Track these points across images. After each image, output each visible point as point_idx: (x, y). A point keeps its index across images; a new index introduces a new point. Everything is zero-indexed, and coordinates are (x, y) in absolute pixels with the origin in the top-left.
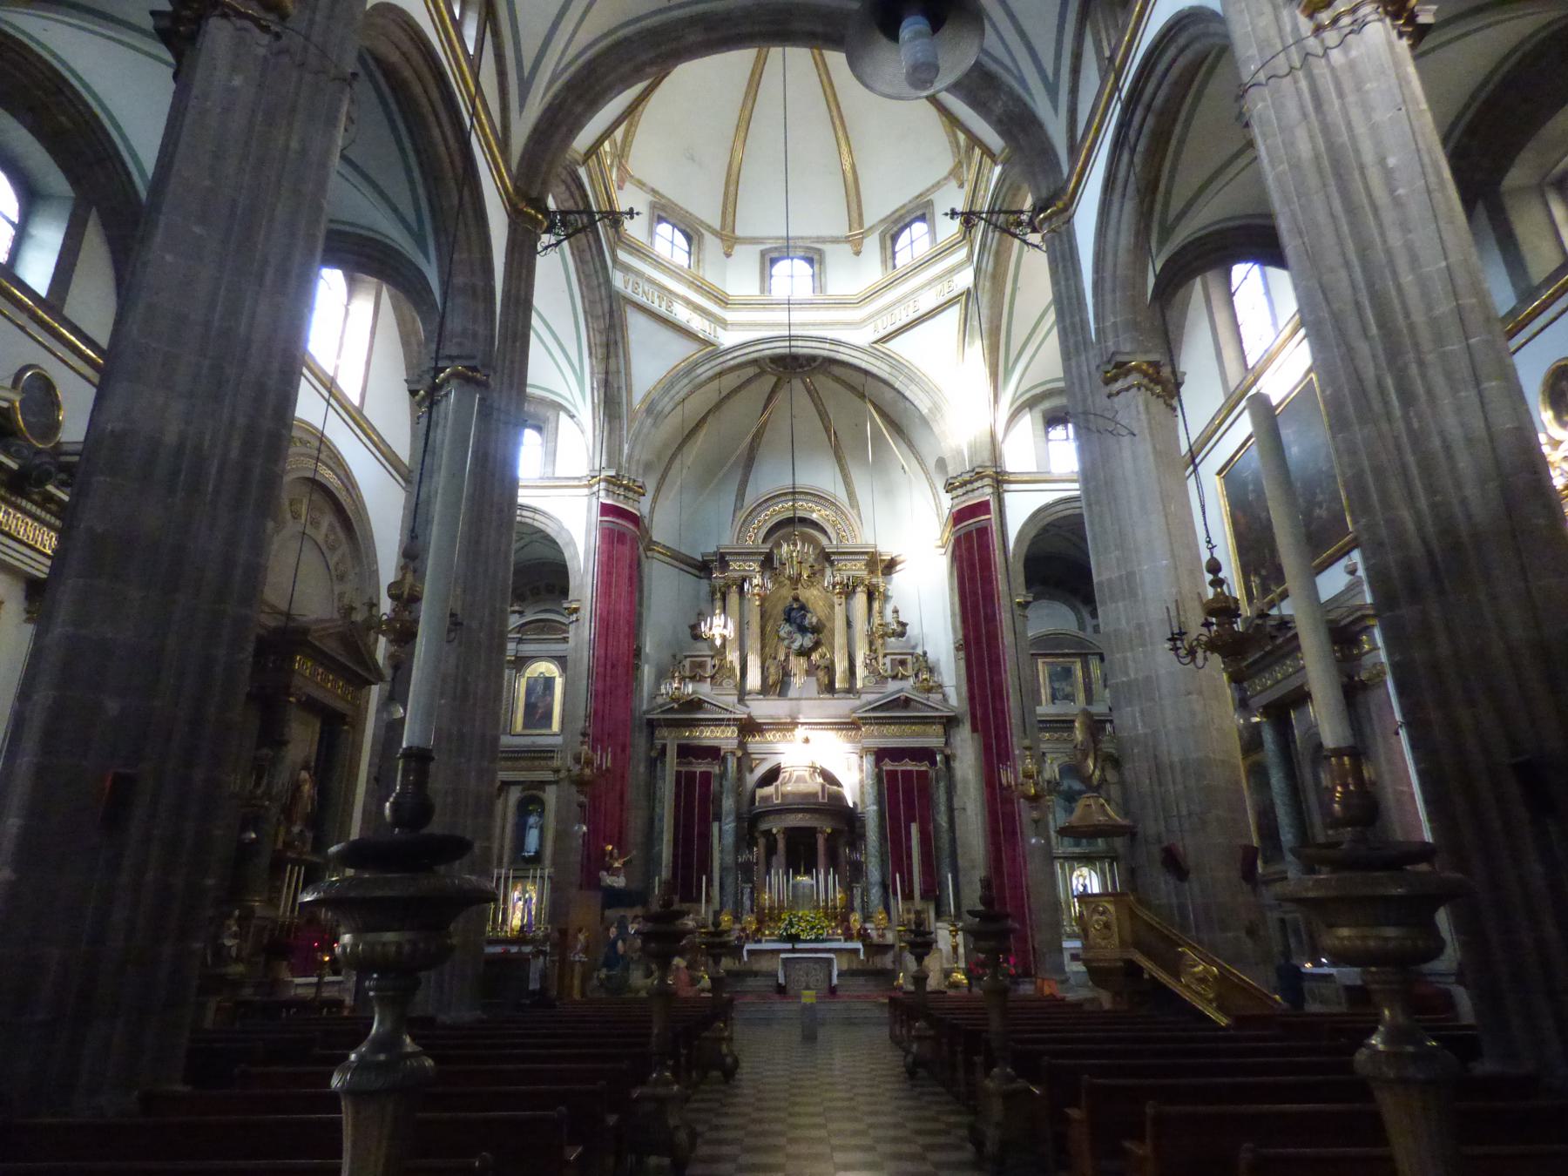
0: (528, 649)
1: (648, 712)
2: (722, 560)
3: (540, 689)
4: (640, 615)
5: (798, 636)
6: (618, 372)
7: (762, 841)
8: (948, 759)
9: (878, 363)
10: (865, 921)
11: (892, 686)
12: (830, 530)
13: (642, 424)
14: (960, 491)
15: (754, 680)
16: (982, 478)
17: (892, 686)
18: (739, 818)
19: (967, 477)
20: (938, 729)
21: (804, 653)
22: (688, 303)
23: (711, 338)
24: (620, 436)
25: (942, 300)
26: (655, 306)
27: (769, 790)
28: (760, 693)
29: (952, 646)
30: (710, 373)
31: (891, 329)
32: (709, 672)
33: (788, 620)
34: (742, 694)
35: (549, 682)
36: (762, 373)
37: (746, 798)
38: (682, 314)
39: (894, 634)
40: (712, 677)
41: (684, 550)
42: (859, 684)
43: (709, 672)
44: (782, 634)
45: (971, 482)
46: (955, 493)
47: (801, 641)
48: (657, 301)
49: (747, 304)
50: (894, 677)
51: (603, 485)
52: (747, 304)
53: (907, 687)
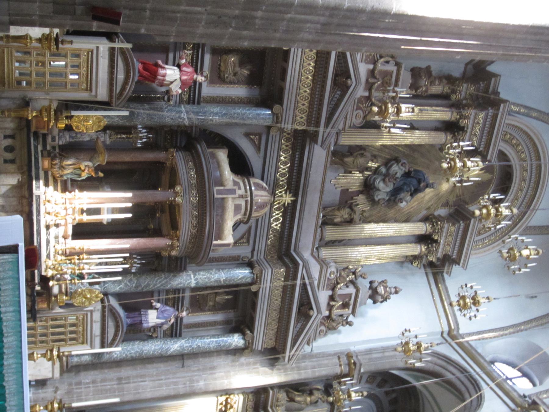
2: (489, 101)
5: (389, 188)
11: (323, 296)
17: (323, 296)
20: (271, 344)
21: (368, 187)
33: (407, 175)
40: (369, 98)
47: (384, 189)
50: (332, 298)
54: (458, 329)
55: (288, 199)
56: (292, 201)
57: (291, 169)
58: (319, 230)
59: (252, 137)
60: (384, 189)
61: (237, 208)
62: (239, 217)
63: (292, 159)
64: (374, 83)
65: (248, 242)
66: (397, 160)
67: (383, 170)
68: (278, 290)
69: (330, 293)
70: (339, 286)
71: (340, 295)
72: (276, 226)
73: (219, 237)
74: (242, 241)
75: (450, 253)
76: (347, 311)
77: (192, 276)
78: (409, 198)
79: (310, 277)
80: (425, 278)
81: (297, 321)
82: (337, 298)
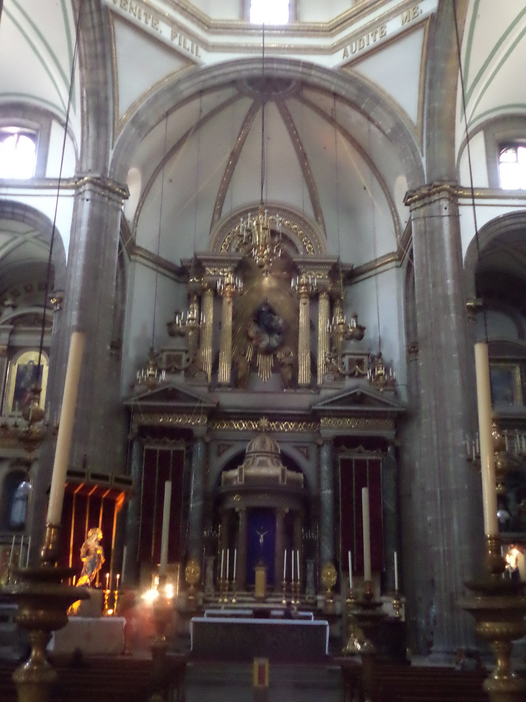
0: (20, 339)
1: (127, 399)
2: (198, 265)
3: (28, 376)
4: (123, 312)
6: (106, 83)
7: (225, 520)
8: (398, 452)
9: (347, 86)
10: (316, 593)
11: (349, 383)
12: (297, 242)
13: (127, 133)
14: (418, 204)
15: (225, 374)
16: (439, 192)
17: (349, 383)
18: (205, 498)
19: (425, 191)
20: (390, 423)
21: (269, 351)
22: (172, 22)
23: (193, 56)
24: (106, 142)
25: (407, 25)
26: (142, 22)
27: (235, 473)
28: (229, 386)
29: (405, 349)
30: (192, 90)
31: (358, 53)
32: (184, 364)
34: (215, 385)
35: (38, 370)
36: (240, 95)
37: (212, 482)
38: (165, 32)
39: (352, 337)
40: (186, 370)
41: (164, 255)
42: (319, 381)
43: (184, 364)
44: (251, 334)
45: (429, 195)
46: (413, 206)
47: (266, 341)
48: (143, 18)
49: (226, 28)
50: (352, 375)
51: (87, 186)
52: (226, 28)
53: (361, 385)
54: (393, 254)
55: (264, 422)
56: (265, 418)
57: (244, 420)
58: (298, 391)
59: (221, 451)
60: (266, 341)
61: (262, 464)
62: (269, 461)
63: (237, 420)
64: (175, 368)
65: (306, 447)
66: (247, 332)
67: (254, 342)
68: (340, 423)
69: (347, 377)
70: (341, 371)
71: (350, 369)
72: (292, 426)
73: (276, 478)
74: (305, 452)
75: (327, 272)
76: (366, 359)
77: (323, 492)
78: (276, 318)
79: (324, 399)
80: (366, 281)
81: (369, 404)
82: (352, 371)
